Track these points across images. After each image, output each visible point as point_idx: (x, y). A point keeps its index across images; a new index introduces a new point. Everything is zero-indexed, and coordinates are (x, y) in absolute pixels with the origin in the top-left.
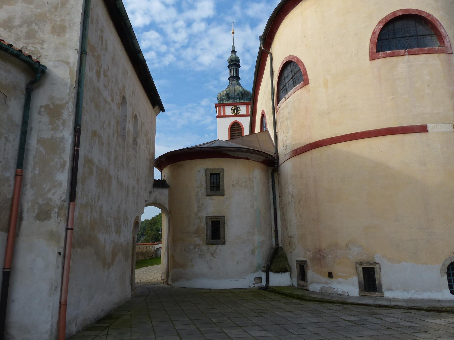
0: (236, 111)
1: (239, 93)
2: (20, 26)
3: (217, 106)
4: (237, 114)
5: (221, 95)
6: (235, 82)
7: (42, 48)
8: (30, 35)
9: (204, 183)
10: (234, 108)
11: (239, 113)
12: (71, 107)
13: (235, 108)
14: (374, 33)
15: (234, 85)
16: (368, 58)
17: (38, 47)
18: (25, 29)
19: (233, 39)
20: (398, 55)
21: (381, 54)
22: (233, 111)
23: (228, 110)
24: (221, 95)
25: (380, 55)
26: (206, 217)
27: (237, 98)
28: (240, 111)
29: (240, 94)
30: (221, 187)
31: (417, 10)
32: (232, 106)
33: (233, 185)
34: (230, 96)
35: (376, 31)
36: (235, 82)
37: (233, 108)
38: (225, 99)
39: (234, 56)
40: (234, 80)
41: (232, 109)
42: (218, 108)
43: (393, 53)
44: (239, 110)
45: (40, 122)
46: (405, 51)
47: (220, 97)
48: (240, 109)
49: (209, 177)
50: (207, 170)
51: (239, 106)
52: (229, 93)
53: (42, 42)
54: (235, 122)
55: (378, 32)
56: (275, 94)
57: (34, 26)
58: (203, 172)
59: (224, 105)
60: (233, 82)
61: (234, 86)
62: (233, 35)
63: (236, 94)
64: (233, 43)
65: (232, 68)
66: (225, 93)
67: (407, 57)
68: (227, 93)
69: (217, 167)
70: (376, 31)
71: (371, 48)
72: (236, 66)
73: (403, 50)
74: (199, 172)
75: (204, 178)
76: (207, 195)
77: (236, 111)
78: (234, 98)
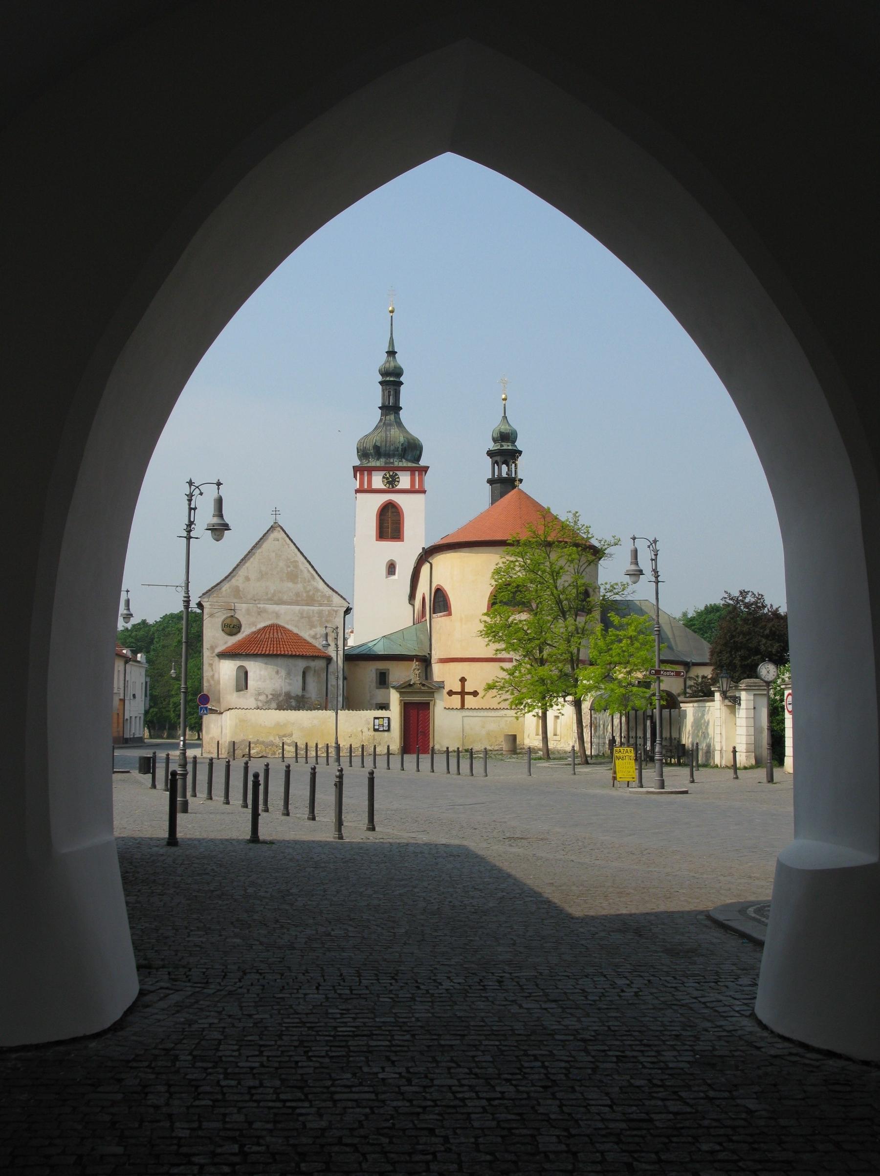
0: (392, 482)
1: (398, 447)
2: (320, 638)
4: (393, 487)
5: (365, 445)
6: (392, 417)
9: (374, 678)
10: (388, 476)
11: (396, 486)
13: (390, 476)
15: (390, 425)
19: (392, 325)
23: (378, 481)
24: (365, 445)
27: (394, 456)
28: (399, 482)
29: (400, 449)
30: (387, 683)
34: (382, 450)
36: (392, 417)
37: (385, 475)
38: (372, 455)
39: (392, 364)
40: (390, 414)
41: (384, 478)
47: (362, 448)
48: (398, 478)
50: (377, 669)
51: (397, 472)
54: (388, 502)
56: (432, 602)
58: (374, 671)
59: (370, 470)
60: (388, 417)
61: (389, 428)
62: (392, 316)
64: (392, 334)
69: (384, 668)
72: (393, 385)
74: (371, 671)
76: (377, 688)
77: (392, 482)
78: (388, 455)
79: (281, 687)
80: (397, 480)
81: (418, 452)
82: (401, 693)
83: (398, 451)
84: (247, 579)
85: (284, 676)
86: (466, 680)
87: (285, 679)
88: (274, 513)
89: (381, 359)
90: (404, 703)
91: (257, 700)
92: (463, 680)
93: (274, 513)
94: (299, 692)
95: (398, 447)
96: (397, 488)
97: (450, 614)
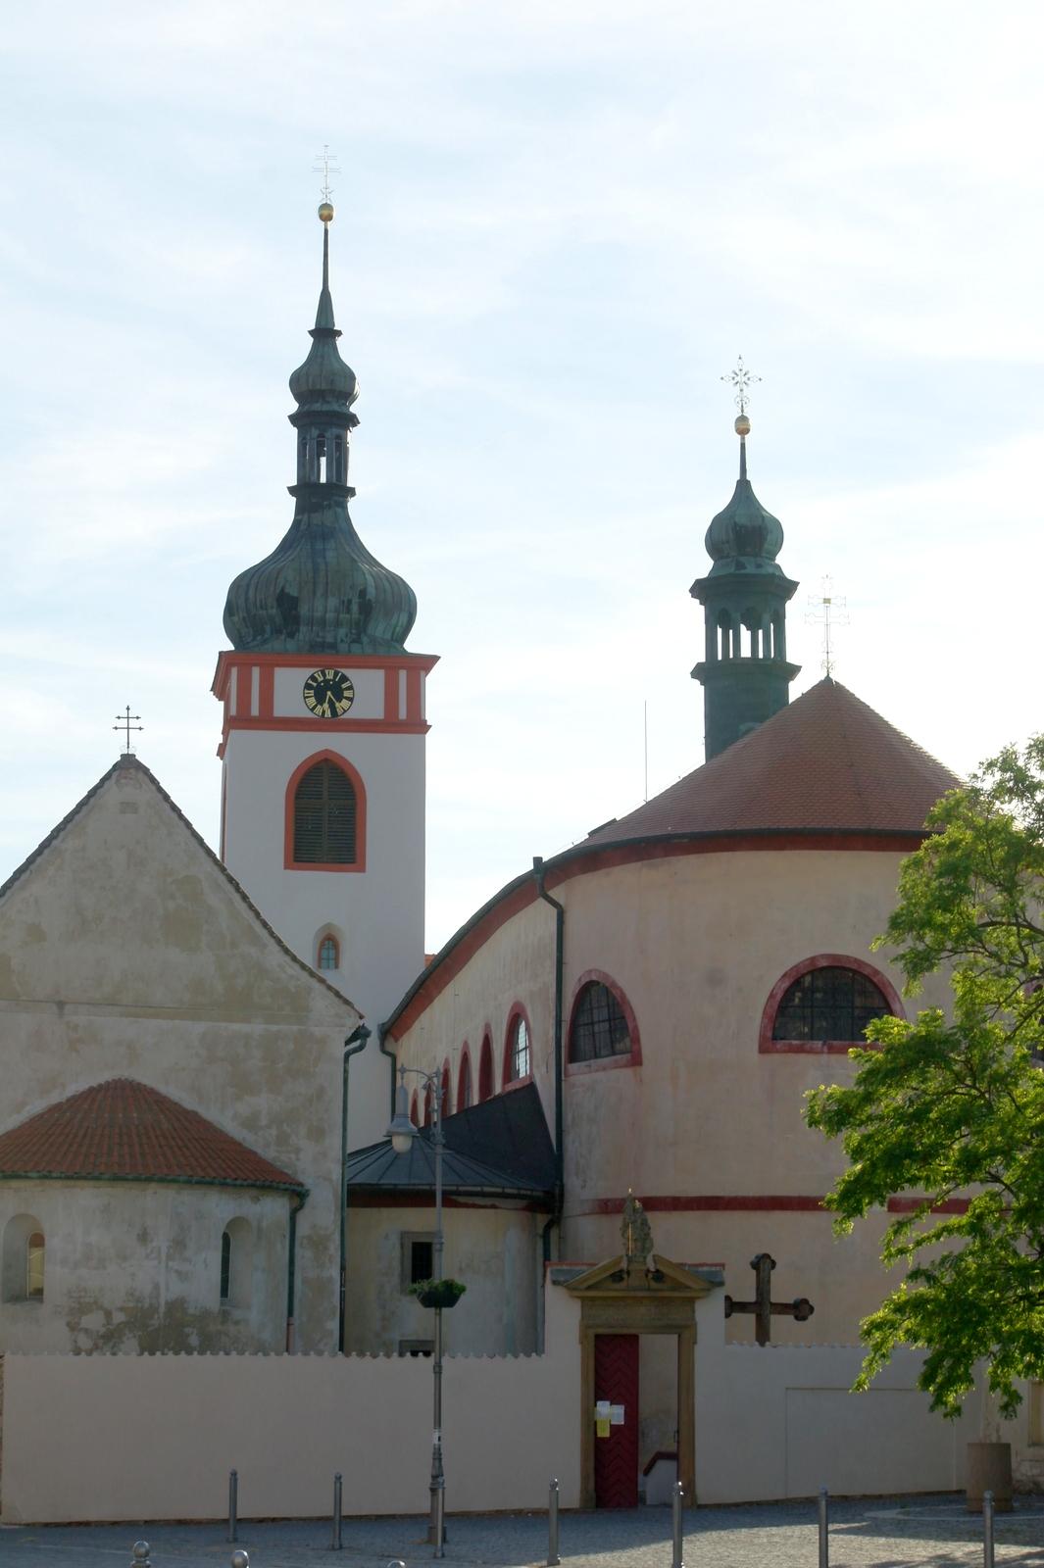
3: (233, 665)
7: (298, 1159)
8: (282, 1140)
9: (396, 1264)
12: (337, 1237)
14: (772, 996)
16: (756, 1047)
17: (293, 1156)
18: (274, 1132)
20: (811, 1051)
21: (780, 1044)
22: (316, 696)
23: (290, 689)
25: (778, 1046)
26: (401, 1342)
27: (338, 624)
28: (351, 699)
29: (355, 608)
31: (856, 960)
32: (310, 671)
33: (461, 1269)
35: (777, 994)
37: (313, 678)
41: (308, 686)
43: (802, 1045)
44: (347, 694)
45: (303, 1257)
46: (824, 1044)
49: (409, 1252)
50: (403, 1235)
51: (347, 672)
52: (296, 595)
53: (298, 1151)
55: (779, 997)
57: (285, 1127)
58: (395, 1240)
66: (278, 591)
67: (825, 1057)
70: (777, 994)
71: (763, 1029)
73: (821, 1042)
75: (397, 1253)
79: (156, 1287)
80: (347, 694)
81: (404, 618)
82: (587, 1303)
83: (348, 611)
84: (36, 933)
85: (164, 1250)
86: (773, 1264)
87: (169, 1258)
88: (133, 723)
89: (299, 350)
90: (598, 1337)
91: (73, 1327)
92: (763, 1264)
93: (123, 723)
94: (211, 1300)
95: (350, 601)
97: (636, 1060)
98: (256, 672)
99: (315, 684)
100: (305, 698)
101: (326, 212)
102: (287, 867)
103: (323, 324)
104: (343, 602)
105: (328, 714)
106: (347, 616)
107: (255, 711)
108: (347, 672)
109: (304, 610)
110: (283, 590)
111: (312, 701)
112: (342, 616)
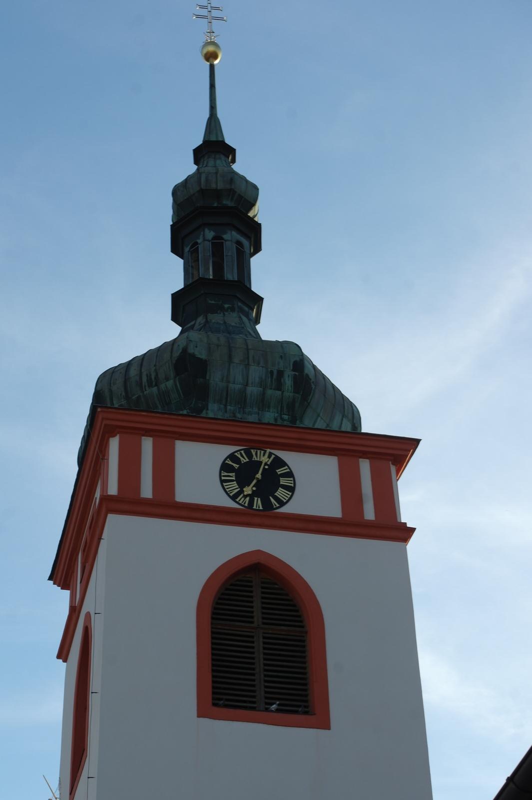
3: (110, 432)
4: (267, 506)
11: (282, 504)
27: (263, 403)
28: (292, 489)
29: (288, 382)
37: (232, 457)
41: (225, 467)
42: (114, 445)
48: (290, 474)
51: (283, 455)
52: (203, 356)
63: (256, 372)
65: (210, 234)
68: (193, 355)
80: (283, 481)
83: (279, 386)
95: (281, 373)
96: (284, 510)
98: (147, 445)
99: (236, 466)
100: (222, 482)
101: (211, 48)
102: (202, 713)
103: (213, 138)
104: (272, 372)
105: (258, 503)
106: (279, 393)
107: (147, 491)
108: (283, 455)
109: (215, 378)
110: (185, 350)
111: (234, 487)
112: (269, 392)
